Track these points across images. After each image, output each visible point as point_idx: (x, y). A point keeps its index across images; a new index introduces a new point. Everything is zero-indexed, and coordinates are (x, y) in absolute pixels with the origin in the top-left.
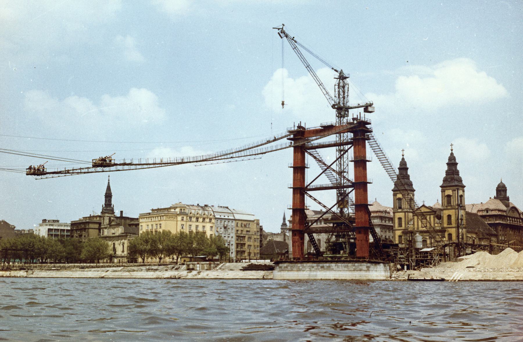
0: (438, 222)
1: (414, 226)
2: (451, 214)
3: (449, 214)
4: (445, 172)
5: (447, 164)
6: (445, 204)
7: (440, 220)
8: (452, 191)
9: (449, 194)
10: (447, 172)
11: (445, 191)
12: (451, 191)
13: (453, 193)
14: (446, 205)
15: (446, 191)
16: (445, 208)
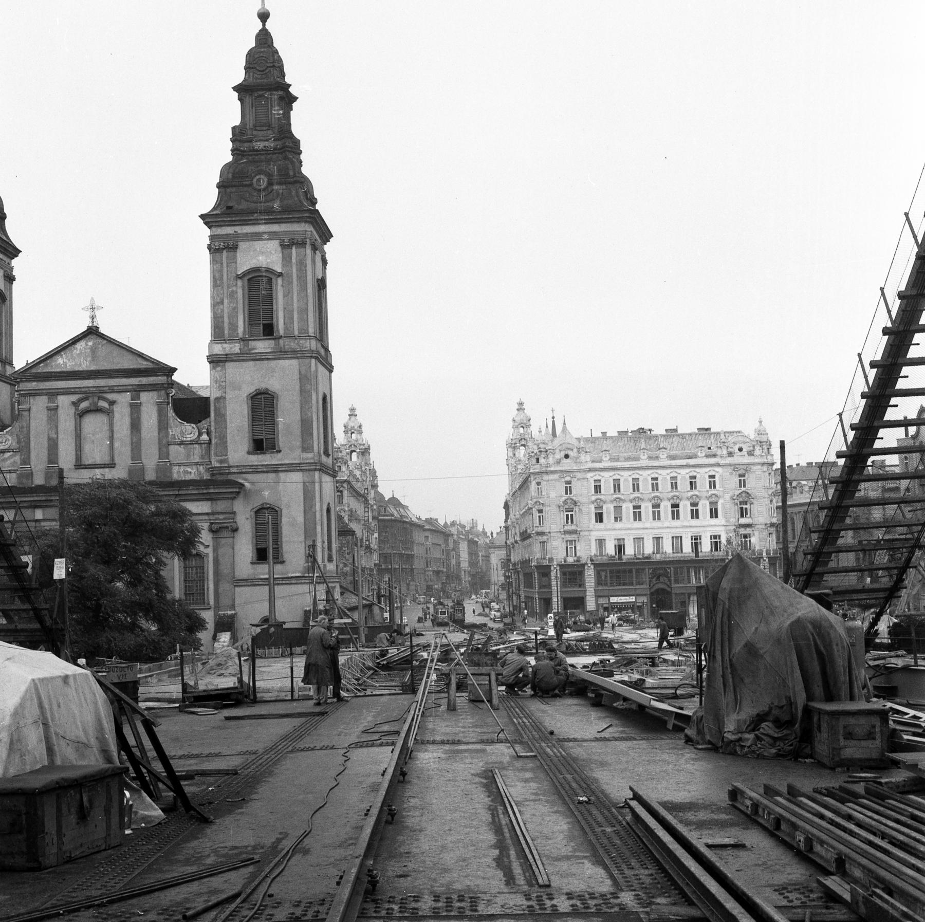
0: (189, 437)
1: (26, 461)
2: (273, 384)
3: (263, 386)
4: (230, 135)
5: (236, 89)
6: (234, 327)
7: (204, 424)
8: (283, 246)
9: (262, 261)
10: (238, 135)
11: (234, 248)
12: (274, 245)
13: (286, 260)
14: (241, 330)
15: (242, 245)
16: (236, 348)
